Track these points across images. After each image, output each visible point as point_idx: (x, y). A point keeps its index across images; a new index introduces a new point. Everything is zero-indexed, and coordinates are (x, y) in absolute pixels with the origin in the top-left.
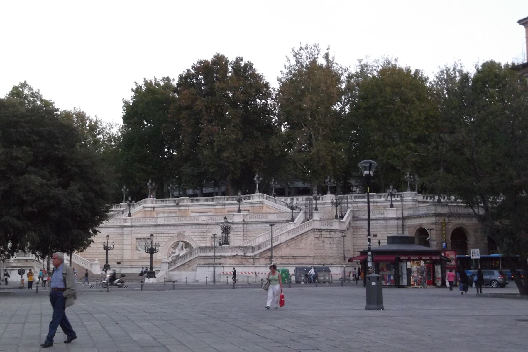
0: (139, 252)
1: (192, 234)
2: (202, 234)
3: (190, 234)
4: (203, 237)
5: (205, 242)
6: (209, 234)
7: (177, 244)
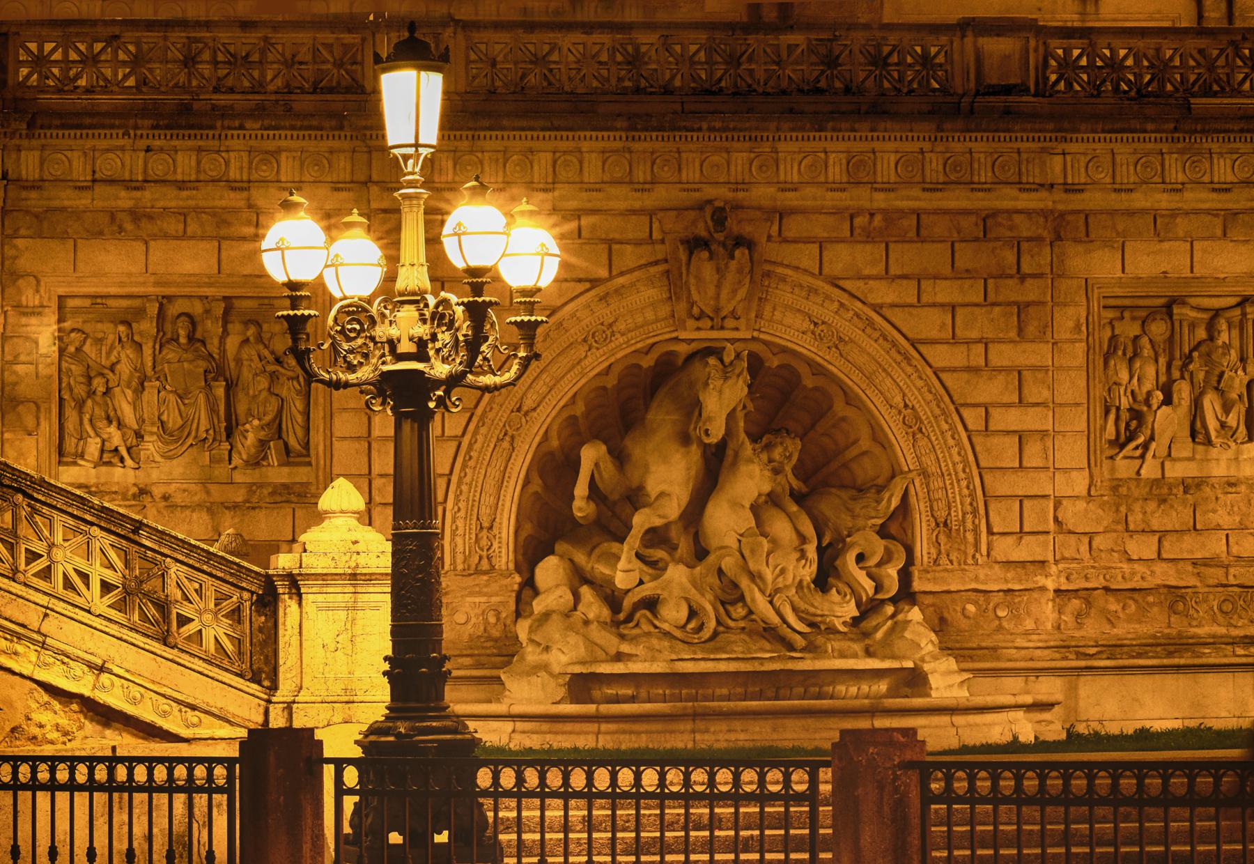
1: (865, 257)
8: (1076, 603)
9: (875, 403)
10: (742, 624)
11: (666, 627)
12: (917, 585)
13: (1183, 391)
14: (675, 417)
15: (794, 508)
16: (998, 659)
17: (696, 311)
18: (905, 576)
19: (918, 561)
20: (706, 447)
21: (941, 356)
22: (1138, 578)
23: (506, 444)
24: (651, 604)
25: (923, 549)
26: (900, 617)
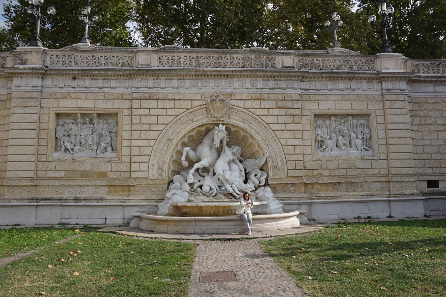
0: (68, 156)
1: (256, 104)
2: (290, 104)
3: (248, 104)
4: (291, 112)
5: (299, 127)
6: (307, 105)
7: (205, 132)
8: (310, 186)
9: (258, 138)
10: (223, 192)
11: (204, 193)
12: (270, 182)
13: (334, 135)
14: (208, 142)
15: (239, 163)
16: (290, 200)
17: (213, 116)
18: (267, 179)
19: (270, 176)
20: (215, 148)
21: (274, 127)
22: (325, 180)
23: (166, 148)
24: (201, 187)
25: (271, 174)
26: (265, 190)
